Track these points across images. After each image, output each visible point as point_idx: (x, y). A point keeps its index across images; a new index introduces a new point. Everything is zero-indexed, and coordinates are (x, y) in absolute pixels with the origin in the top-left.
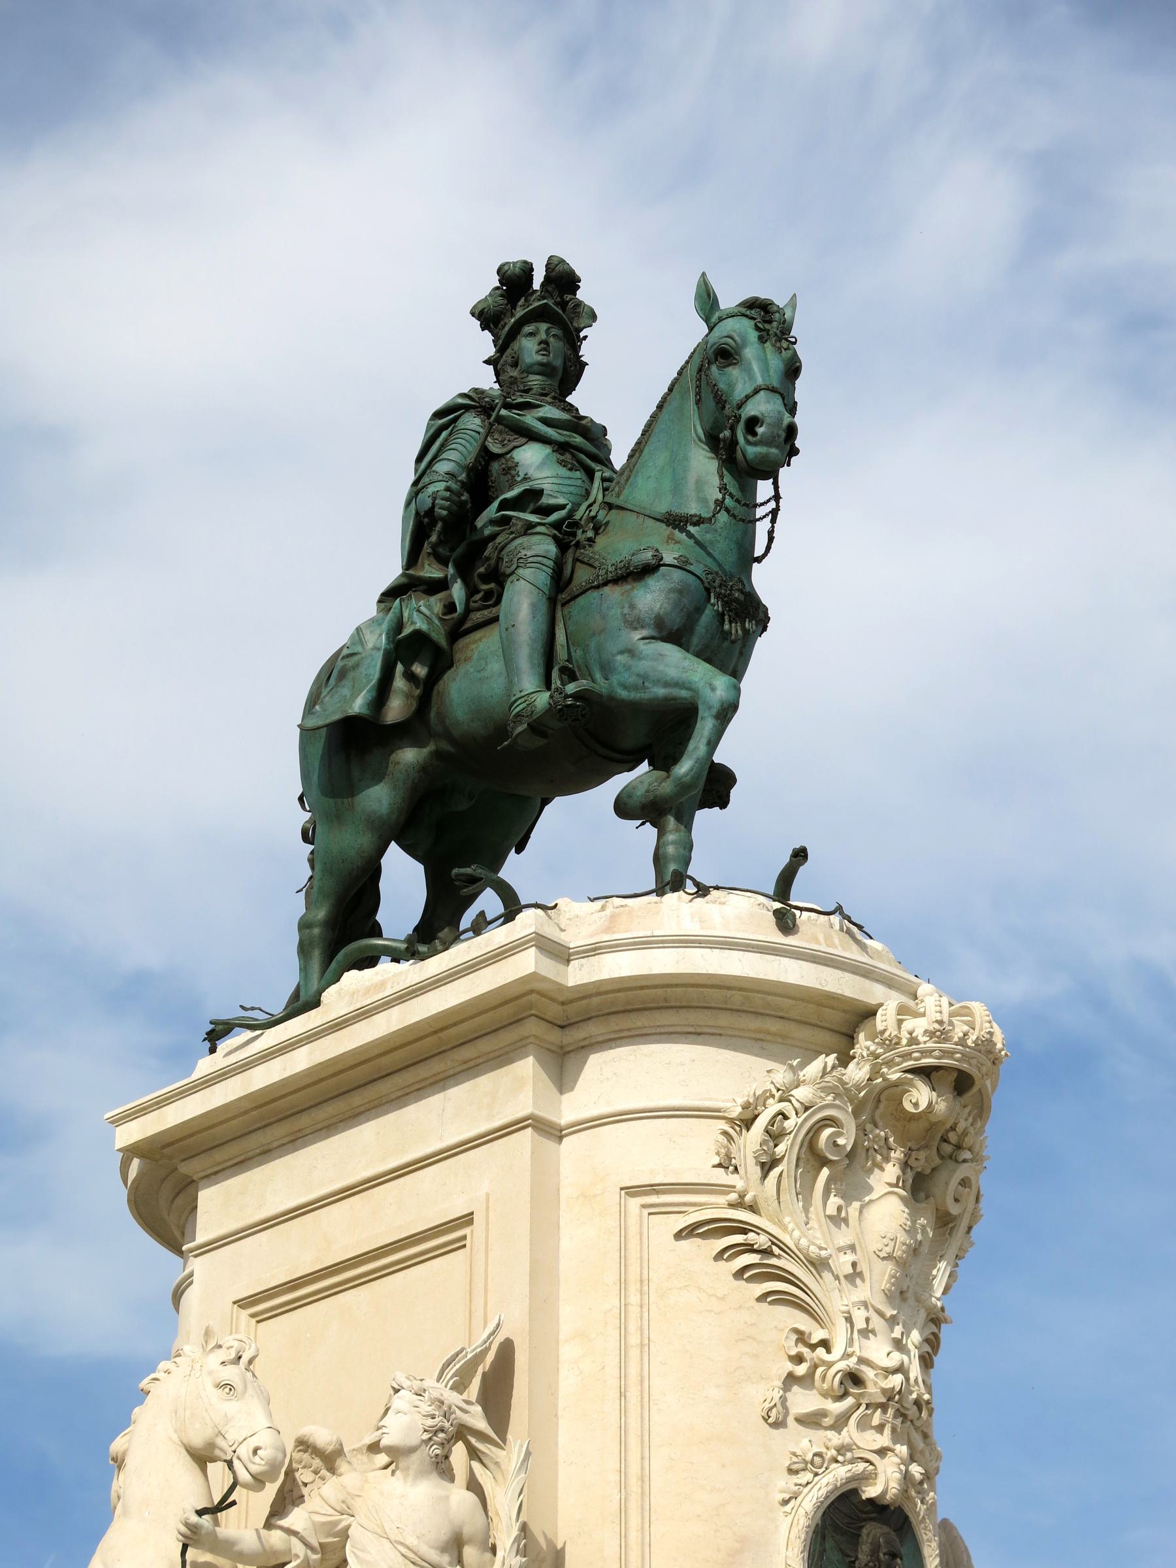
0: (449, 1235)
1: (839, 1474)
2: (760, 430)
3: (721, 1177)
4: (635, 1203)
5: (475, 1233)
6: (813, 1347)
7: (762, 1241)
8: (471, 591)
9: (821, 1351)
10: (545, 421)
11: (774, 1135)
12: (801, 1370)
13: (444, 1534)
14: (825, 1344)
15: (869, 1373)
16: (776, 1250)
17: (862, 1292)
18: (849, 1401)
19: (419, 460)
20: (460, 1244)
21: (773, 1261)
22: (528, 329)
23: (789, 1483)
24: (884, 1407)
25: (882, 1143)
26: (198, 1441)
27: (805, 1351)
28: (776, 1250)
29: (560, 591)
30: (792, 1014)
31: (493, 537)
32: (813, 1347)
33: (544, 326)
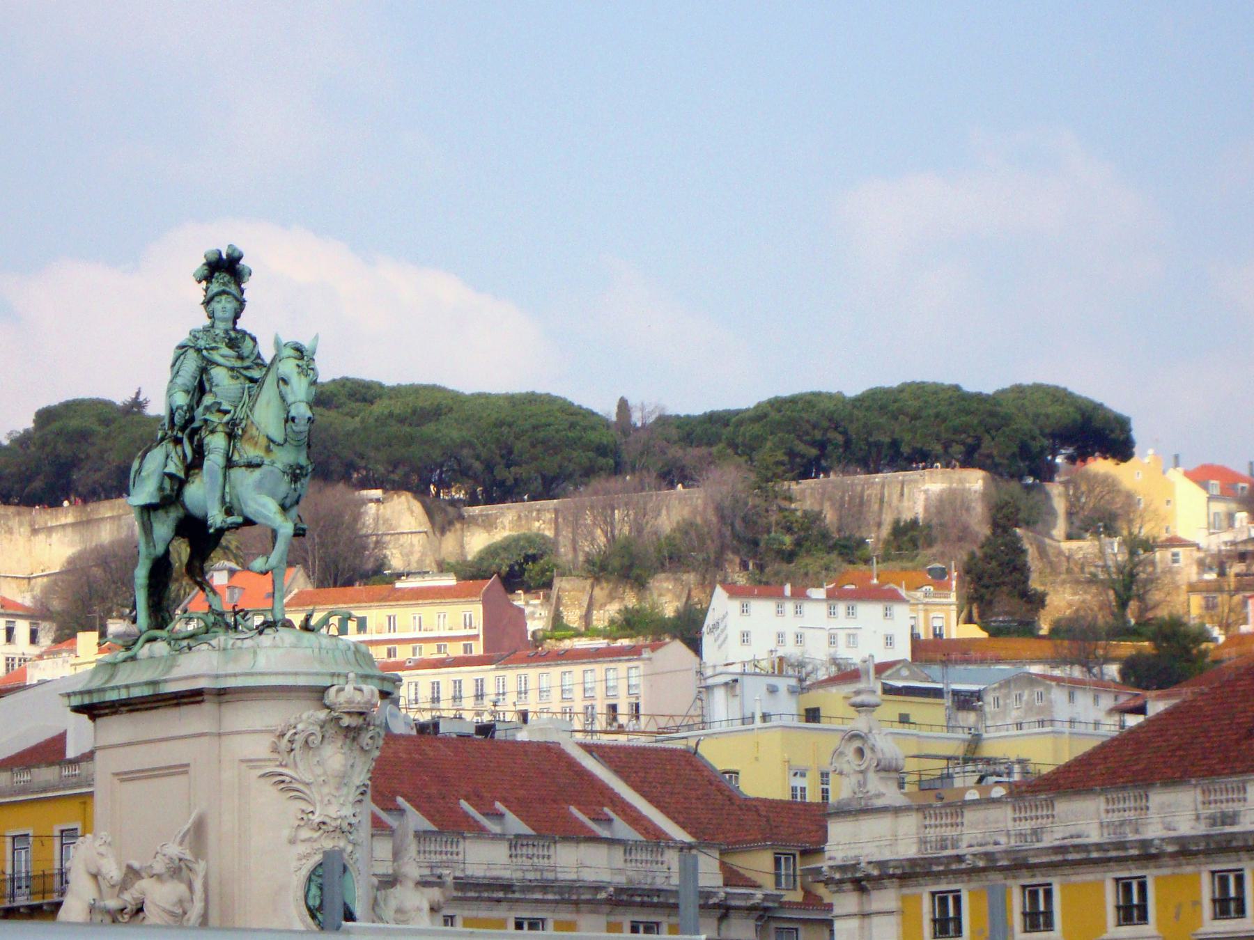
0: (181, 769)
3: (275, 756)
4: (245, 765)
5: (192, 770)
7: (288, 779)
8: (194, 451)
10: (223, 356)
11: (291, 742)
13: (175, 899)
15: (327, 820)
17: (326, 790)
19: (173, 365)
20: (186, 772)
22: (217, 299)
26: (94, 871)
27: (305, 816)
29: (230, 464)
31: (200, 428)
33: (224, 297)
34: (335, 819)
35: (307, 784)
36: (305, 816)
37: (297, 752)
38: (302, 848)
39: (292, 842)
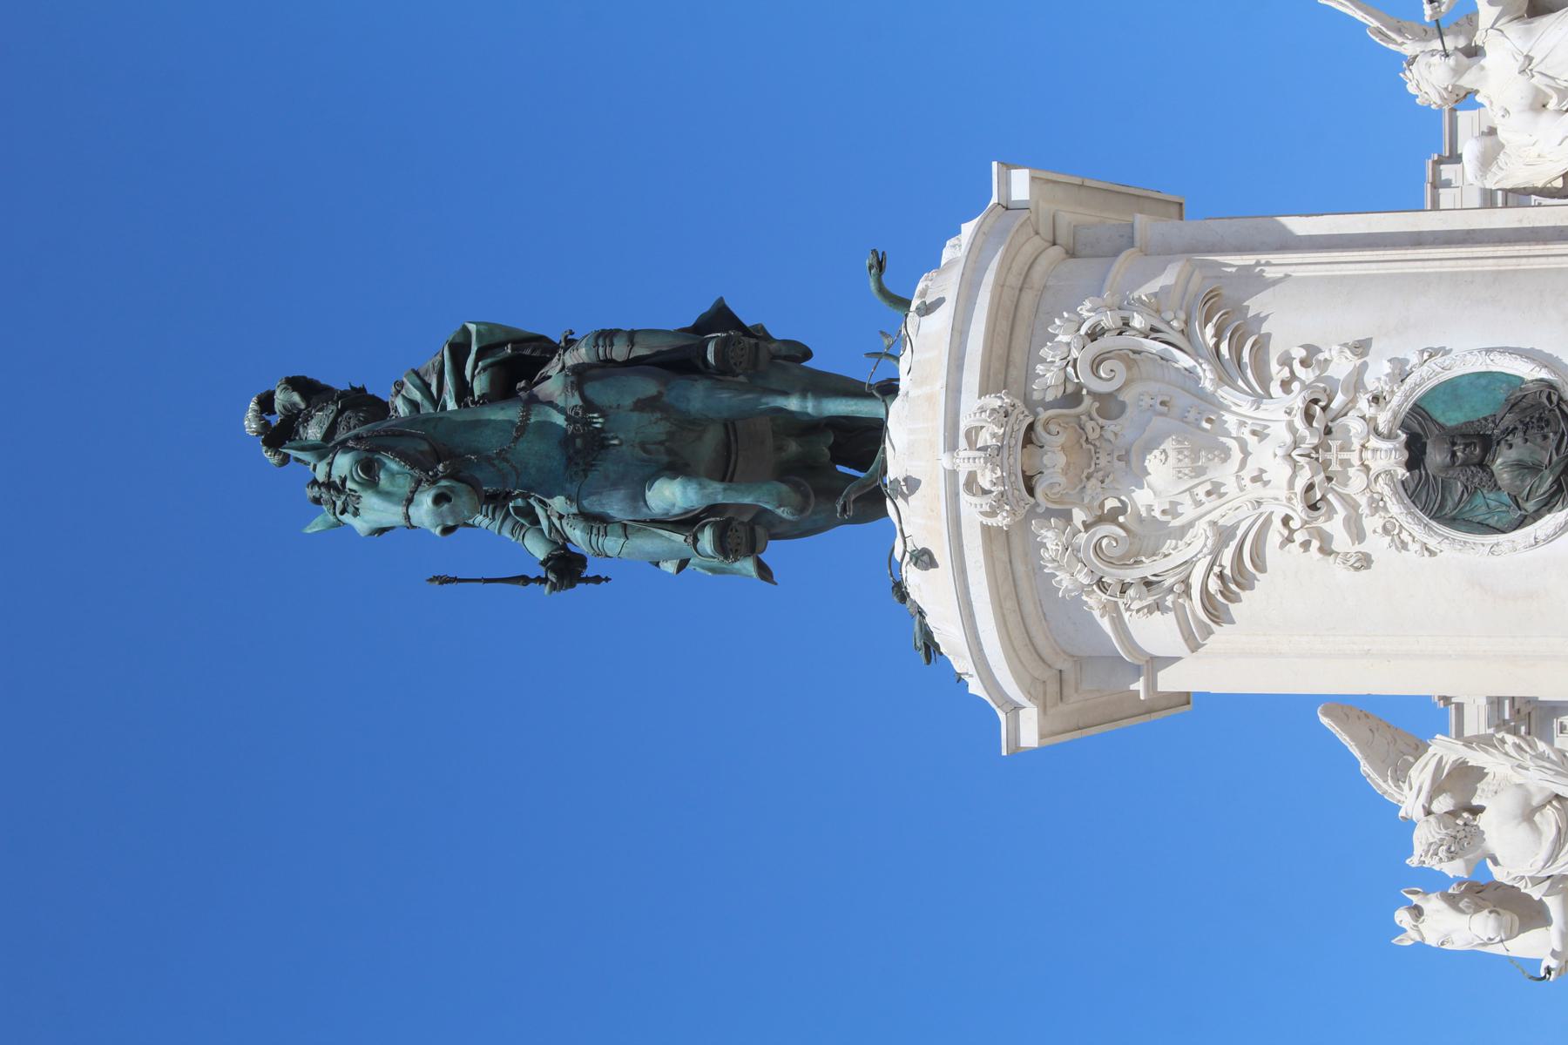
1: (1395, 508)
2: (450, 523)
6: (1292, 531)
7: (1214, 585)
9: (1294, 524)
12: (1315, 544)
14: (1286, 521)
15: (1300, 484)
16: (1216, 569)
18: (1330, 497)
21: (1228, 572)
23: (1413, 547)
24: (1326, 465)
25: (1093, 481)
27: (1299, 537)
28: (1216, 569)
30: (1005, 558)
32: (1292, 531)
34: (1295, 466)
35: (1224, 535)
36: (1299, 537)
37: (1148, 569)
38: (1376, 544)
39: (1365, 561)
